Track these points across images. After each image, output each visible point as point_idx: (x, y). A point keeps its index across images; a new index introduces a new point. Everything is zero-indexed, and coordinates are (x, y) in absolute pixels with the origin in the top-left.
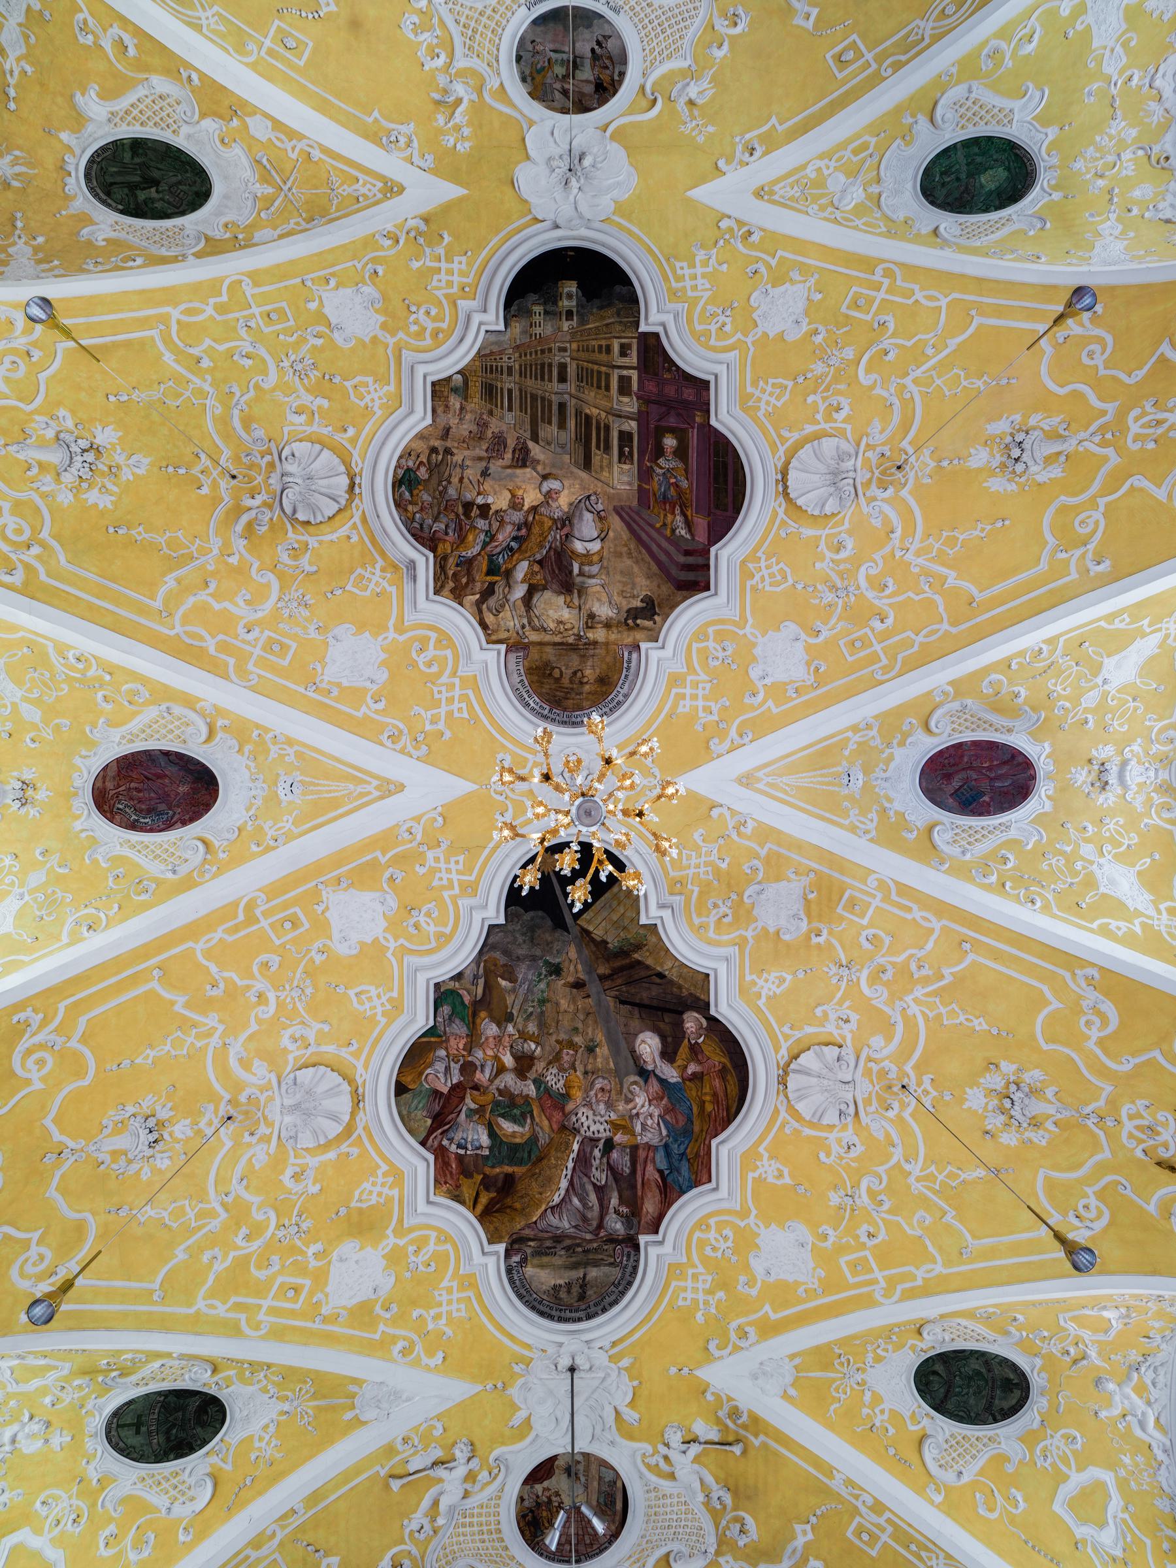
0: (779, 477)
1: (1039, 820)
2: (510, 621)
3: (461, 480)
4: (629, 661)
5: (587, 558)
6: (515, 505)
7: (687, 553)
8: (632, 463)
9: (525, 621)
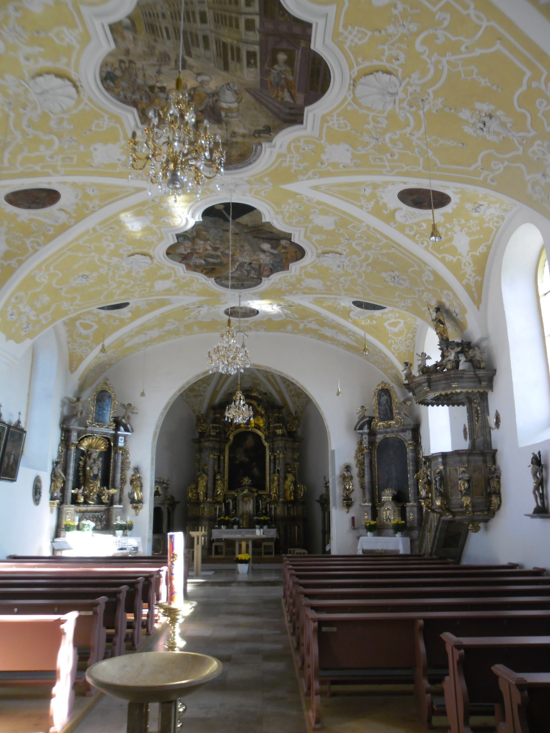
0: (352, 82)
1: (444, 215)
3: (144, 76)
4: (256, 149)
5: (230, 110)
7: (291, 108)
8: (256, 67)
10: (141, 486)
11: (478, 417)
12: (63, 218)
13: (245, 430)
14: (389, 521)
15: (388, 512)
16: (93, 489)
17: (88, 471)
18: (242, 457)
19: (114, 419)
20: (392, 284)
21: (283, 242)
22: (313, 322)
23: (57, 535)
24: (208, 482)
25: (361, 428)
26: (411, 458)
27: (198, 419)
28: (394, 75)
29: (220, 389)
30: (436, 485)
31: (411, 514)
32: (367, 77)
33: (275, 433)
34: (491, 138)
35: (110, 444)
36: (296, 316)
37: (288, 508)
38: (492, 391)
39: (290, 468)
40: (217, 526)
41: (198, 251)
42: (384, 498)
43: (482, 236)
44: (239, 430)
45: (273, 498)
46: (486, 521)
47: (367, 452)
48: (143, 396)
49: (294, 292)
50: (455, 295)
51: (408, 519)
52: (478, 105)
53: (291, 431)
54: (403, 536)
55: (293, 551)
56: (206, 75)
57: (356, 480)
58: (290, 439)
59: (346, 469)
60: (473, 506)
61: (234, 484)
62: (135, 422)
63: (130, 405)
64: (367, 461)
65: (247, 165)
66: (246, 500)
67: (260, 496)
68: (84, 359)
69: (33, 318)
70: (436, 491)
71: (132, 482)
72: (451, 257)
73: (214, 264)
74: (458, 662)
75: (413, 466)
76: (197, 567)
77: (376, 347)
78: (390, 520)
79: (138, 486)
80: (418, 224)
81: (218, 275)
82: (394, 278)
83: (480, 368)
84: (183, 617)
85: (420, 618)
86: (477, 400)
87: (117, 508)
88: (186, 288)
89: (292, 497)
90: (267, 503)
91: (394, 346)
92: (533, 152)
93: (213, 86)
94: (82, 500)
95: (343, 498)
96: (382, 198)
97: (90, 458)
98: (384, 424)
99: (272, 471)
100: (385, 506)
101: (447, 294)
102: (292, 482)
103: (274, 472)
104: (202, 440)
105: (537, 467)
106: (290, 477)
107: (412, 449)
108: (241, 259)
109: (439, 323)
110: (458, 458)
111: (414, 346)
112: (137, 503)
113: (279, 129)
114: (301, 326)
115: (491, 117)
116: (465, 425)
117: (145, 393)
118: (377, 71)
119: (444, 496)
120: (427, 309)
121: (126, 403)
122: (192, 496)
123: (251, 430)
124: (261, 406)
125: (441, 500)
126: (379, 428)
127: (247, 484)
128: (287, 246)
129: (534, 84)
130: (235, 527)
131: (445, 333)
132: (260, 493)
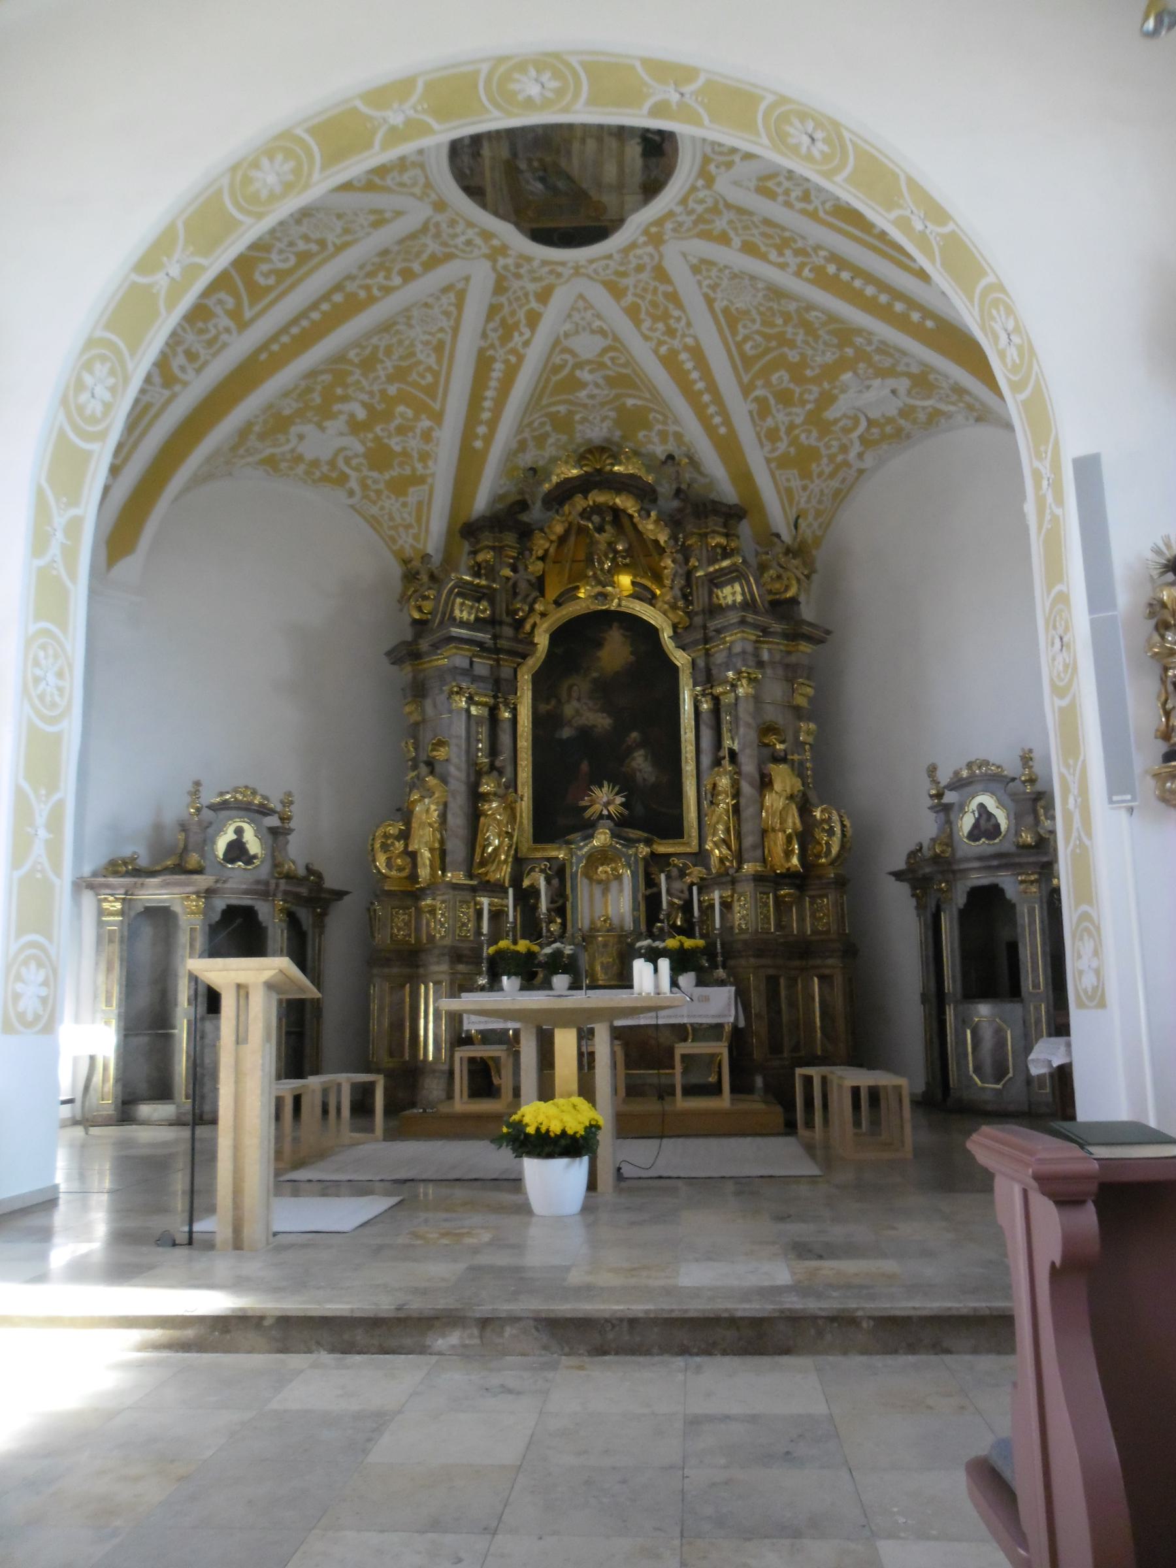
27: (410, 576)
29: (489, 439)
33: (714, 610)
37: (778, 901)
39: (782, 742)
40: (482, 981)
45: (714, 862)
53: (778, 597)
55: (824, 1080)
58: (777, 627)
66: (603, 876)
67: (657, 861)
76: (237, 1192)
89: (795, 861)
90: (693, 884)
95: (1162, 747)
99: (706, 760)
103: (717, 762)
104: (424, 645)
106: (784, 780)
122: (389, 865)
123: (619, 605)
127: (605, 812)
132: (662, 848)
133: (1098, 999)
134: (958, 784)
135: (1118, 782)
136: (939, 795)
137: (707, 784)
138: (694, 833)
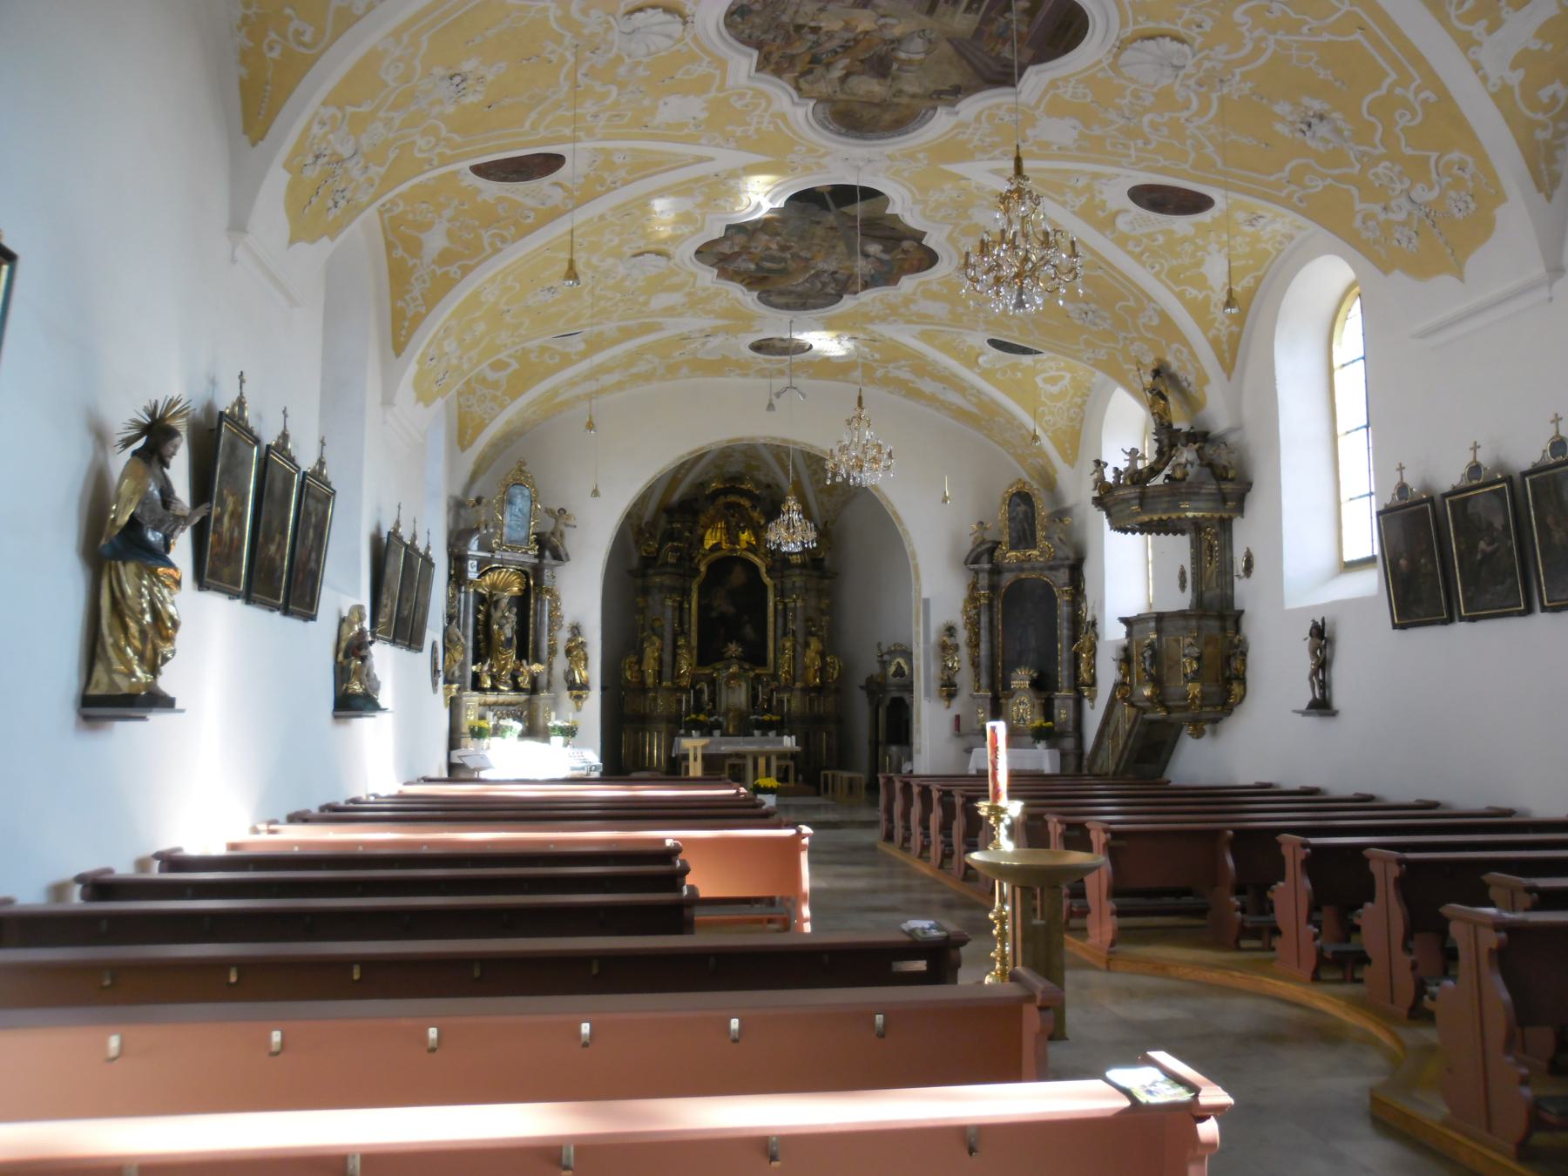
0: (1118, 44)
1: (1197, 225)
2: (823, 88)
4: (925, 114)
5: (910, 62)
6: (847, 27)
9: (838, 89)
10: (586, 659)
11: (1211, 556)
12: (557, 196)
13: (728, 554)
14: (1022, 722)
15: (1021, 707)
16: (506, 664)
17: (496, 632)
18: (722, 605)
19: (535, 536)
20: (1079, 322)
21: (906, 244)
22: (905, 369)
23: (454, 742)
24: (662, 650)
25: (976, 561)
26: (1065, 616)
27: (640, 532)
28: (1188, 44)
30: (1145, 664)
31: (1063, 711)
32: (1146, 42)
34: (1312, 144)
35: (528, 583)
36: (877, 356)
38: (1243, 517)
39: (814, 626)
40: (682, 731)
41: (753, 250)
42: (1015, 684)
43: (1251, 262)
44: (718, 554)
46: (1215, 721)
47: (985, 604)
48: (595, 496)
49: (892, 318)
50: (1193, 354)
51: (1057, 719)
52: (1306, 101)
54: (1050, 746)
55: (833, 776)
56: (894, 17)
57: (964, 652)
59: (947, 633)
60: (1203, 698)
61: (708, 654)
62: (571, 543)
63: (562, 511)
64: (984, 619)
65: (899, 135)
68: (487, 425)
69: (454, 362)
70: (1145, 674)
71: (568, 652)
72: (1195, 292)
73: (770, 271)
74: (1303, 862)
75: (1069, 629)
77: (1015, 418)
78: (1024, 721)
79: (580, 659)
80: (1152, 237)
81: (768, 288)
82: (1086, 313)
83: (1226, 479)
84: (1010, 817)
85: (1228, 829)
86: (1213, 527)
87: (545, 698)
88: (700, 306)
89: (818, 680)
91: (1047, 418)
92: (1376, 175)
93: (897, 31)
94: (488, 683)
95: (940, 683)
96: (1101, 192)
97: (496, 608)
98: (1019, 554)
99: (780, 632)
100: (1016, 695)
101: (1178, 350)
102: (817, 653)
103: (785, 634)
104: (651, 571)
105: (1318, 641)
106: (815, 644)
107: (1067, 601)
108: (821, 266)
109: (1158, 397)
110: (1181, 623)
111: (1082, 419)
112: (578, 689)
113: (977, 89)
114: (880, 373)
115: (1321, 118)
116: (1182, 567)
117: (601, 490)
118: (1163, 36)
119: (1157, 681)
120: (1136, 368)
121: (556, 509)
122: (632, 677)
124: (758, 509)
125: (1153, 687)
126: (1009, 562)
128: (911, 249)
129: (1398, 91)
130: (717, 733)
131: (1166, 414)
133: (919, 752)
134: (890, 653)
135: (927, 694)
136: (882, 656)
137: (780, 644)
138: (772, 664)
